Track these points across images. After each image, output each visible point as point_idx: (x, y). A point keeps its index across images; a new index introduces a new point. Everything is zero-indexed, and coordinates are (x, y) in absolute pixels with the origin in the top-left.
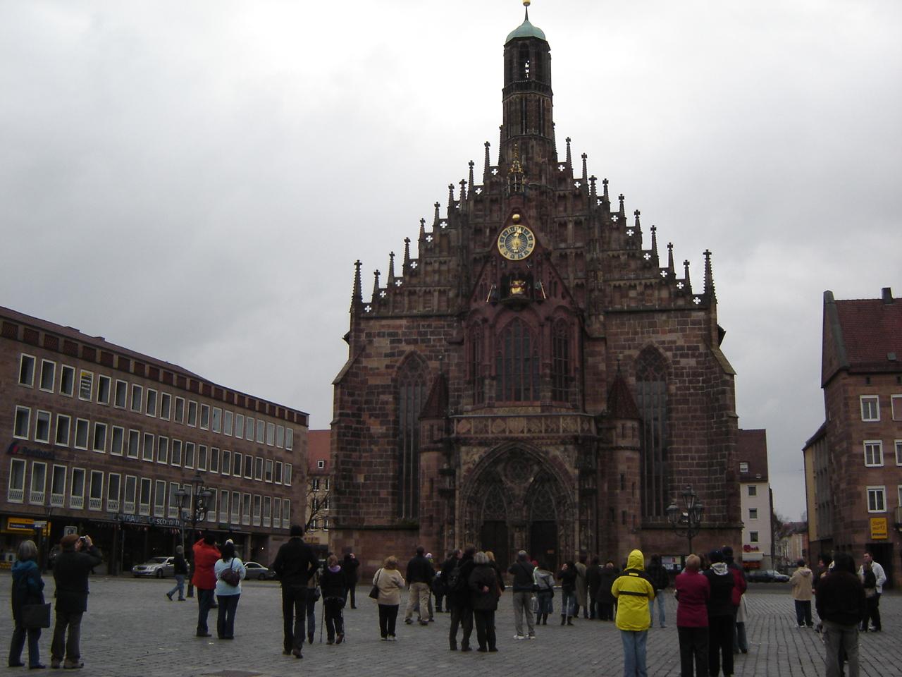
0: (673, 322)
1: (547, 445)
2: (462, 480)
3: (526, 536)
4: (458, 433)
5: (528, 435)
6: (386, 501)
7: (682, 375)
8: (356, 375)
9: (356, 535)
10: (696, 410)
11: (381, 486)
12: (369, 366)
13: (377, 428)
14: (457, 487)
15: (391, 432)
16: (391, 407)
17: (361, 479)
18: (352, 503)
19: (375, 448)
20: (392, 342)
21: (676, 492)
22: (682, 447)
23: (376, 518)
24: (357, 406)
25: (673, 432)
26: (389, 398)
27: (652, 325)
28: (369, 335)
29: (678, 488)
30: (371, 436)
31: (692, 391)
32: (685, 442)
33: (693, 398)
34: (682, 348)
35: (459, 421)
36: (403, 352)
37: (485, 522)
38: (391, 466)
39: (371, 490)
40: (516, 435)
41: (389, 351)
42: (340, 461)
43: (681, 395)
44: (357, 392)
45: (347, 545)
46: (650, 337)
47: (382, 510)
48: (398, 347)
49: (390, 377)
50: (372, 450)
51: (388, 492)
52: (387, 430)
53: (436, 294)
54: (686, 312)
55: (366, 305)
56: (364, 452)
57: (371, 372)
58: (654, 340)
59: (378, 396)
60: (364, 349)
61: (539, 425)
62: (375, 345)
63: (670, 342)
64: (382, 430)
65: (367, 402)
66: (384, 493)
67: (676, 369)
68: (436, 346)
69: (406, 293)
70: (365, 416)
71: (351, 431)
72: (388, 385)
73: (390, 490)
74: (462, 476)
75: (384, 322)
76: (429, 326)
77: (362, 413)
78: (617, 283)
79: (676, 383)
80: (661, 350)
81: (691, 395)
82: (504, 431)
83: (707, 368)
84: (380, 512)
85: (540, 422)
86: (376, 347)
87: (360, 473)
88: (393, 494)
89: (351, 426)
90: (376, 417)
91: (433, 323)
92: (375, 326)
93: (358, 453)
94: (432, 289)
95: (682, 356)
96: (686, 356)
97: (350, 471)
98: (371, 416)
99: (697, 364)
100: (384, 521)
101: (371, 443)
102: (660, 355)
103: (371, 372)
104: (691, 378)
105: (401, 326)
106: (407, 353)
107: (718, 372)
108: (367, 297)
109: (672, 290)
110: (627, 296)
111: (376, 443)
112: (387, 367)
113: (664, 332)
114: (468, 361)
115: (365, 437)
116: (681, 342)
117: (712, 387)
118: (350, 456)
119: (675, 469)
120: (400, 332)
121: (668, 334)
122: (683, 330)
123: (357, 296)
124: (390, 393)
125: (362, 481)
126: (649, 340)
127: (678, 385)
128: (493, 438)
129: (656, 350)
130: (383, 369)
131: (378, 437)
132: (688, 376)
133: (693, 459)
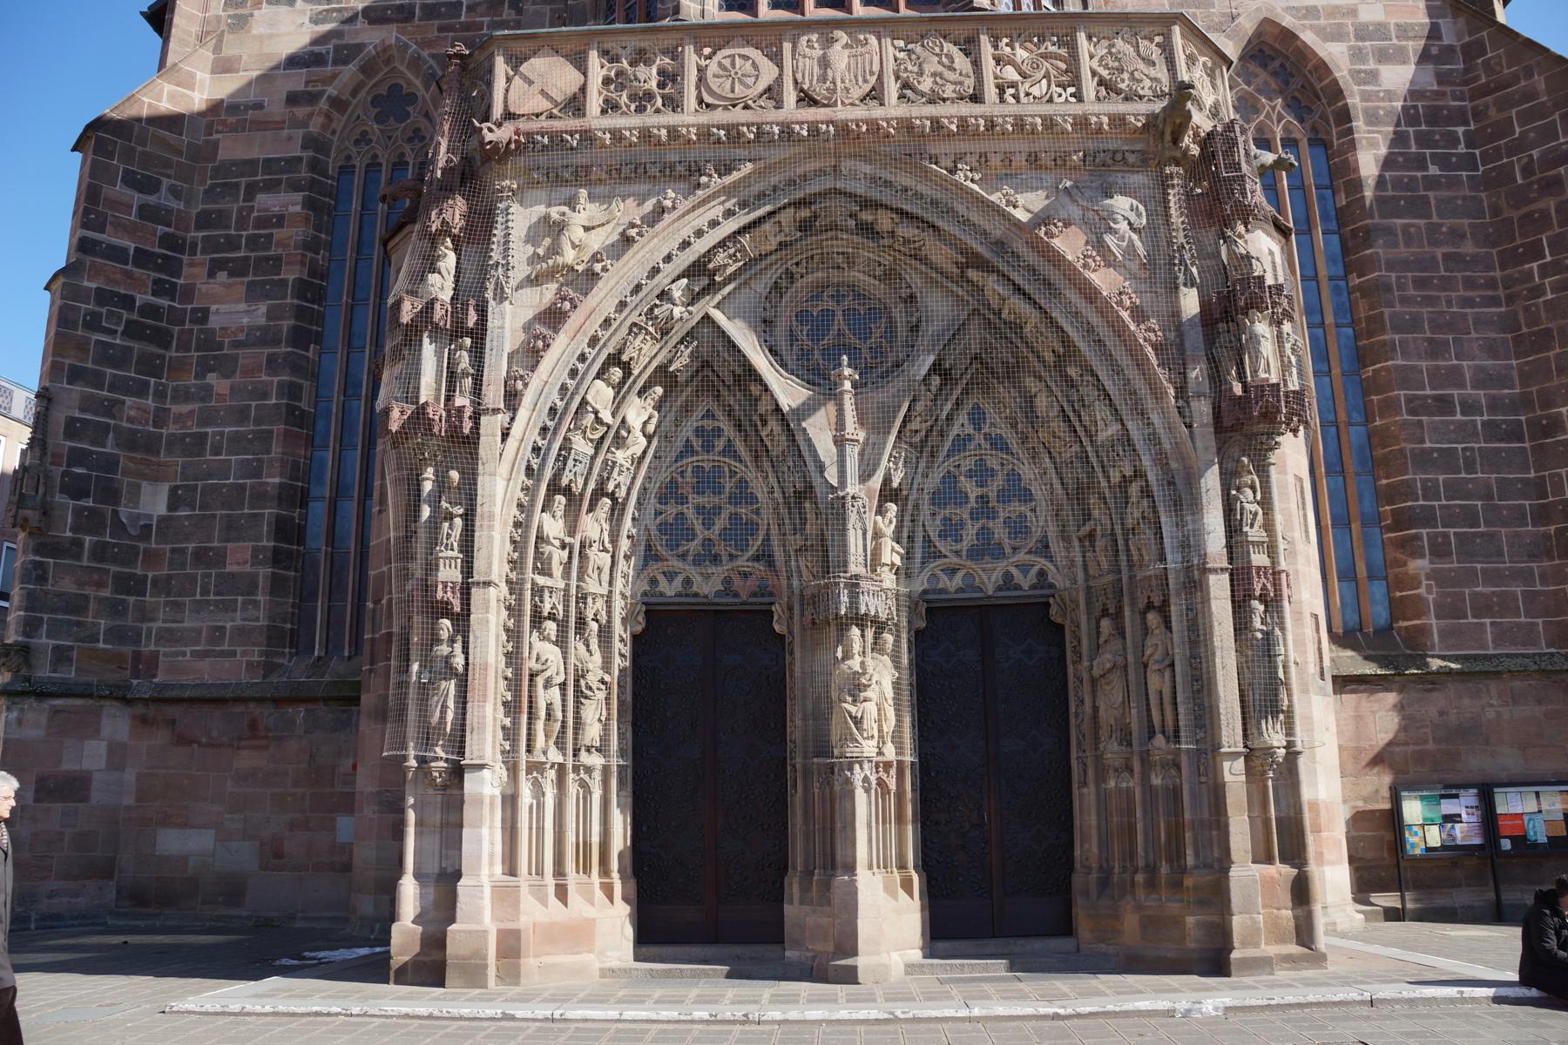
4: (509, 116)
9: (116, 723)
10: (1457, 235)
11: (232, 529)
13: (233, 310)
14: (493, 394)
15: (286, 324)
16: (293, 234)
17: (154, 502)
18: (106, 593)
19: (218, 384)
22: (1424, 364)
25: (1387, 311)
26: (289, 203)
30: (209, 342)
31: (1433, 170)
33: (1445, 194)
34: (1380, 31)
35: (516, 62)
36: (360, 47)
38: (276, 450)
39: (191, 546)
40: (842, 113)
42: (59, 416)
44: (165, 182)
45: (68, 766)
49: (301, 131)
50: (209, 388)
51: (256, 550)
52: (271, 315)
56: (175, 400)
57: (231, 120)
59: (250, 196)
61: (962, 62)
62: (254, 32)
65: (204, 221)
66: (239, 558)
67: (1366, 97)
68: (480, 26)
70: (193, 272)
71: (125, 315)
72: (289, 161)
77: (185, 258)
80: (1308, 37)
81: (1432, 183)
82: (773, 93)
86: (261, 38)
87: (156, 479)
88: (277, 558)
89: (132, 299)
90: (231, 274)
93: (150, 402)
97: (110, 464)
98: (215, 268)
99: (1440, 83)
100: (236, 667)
101: (204, 368)
103: (231, 120)
111: (226, 366)
112: (293, 99)
118: (110, 408)
124: (295, 187)
125: (161, 509)
128: (705, 133)
129: (1288, 36)
131: (237, 344)
133: (1469, 408)
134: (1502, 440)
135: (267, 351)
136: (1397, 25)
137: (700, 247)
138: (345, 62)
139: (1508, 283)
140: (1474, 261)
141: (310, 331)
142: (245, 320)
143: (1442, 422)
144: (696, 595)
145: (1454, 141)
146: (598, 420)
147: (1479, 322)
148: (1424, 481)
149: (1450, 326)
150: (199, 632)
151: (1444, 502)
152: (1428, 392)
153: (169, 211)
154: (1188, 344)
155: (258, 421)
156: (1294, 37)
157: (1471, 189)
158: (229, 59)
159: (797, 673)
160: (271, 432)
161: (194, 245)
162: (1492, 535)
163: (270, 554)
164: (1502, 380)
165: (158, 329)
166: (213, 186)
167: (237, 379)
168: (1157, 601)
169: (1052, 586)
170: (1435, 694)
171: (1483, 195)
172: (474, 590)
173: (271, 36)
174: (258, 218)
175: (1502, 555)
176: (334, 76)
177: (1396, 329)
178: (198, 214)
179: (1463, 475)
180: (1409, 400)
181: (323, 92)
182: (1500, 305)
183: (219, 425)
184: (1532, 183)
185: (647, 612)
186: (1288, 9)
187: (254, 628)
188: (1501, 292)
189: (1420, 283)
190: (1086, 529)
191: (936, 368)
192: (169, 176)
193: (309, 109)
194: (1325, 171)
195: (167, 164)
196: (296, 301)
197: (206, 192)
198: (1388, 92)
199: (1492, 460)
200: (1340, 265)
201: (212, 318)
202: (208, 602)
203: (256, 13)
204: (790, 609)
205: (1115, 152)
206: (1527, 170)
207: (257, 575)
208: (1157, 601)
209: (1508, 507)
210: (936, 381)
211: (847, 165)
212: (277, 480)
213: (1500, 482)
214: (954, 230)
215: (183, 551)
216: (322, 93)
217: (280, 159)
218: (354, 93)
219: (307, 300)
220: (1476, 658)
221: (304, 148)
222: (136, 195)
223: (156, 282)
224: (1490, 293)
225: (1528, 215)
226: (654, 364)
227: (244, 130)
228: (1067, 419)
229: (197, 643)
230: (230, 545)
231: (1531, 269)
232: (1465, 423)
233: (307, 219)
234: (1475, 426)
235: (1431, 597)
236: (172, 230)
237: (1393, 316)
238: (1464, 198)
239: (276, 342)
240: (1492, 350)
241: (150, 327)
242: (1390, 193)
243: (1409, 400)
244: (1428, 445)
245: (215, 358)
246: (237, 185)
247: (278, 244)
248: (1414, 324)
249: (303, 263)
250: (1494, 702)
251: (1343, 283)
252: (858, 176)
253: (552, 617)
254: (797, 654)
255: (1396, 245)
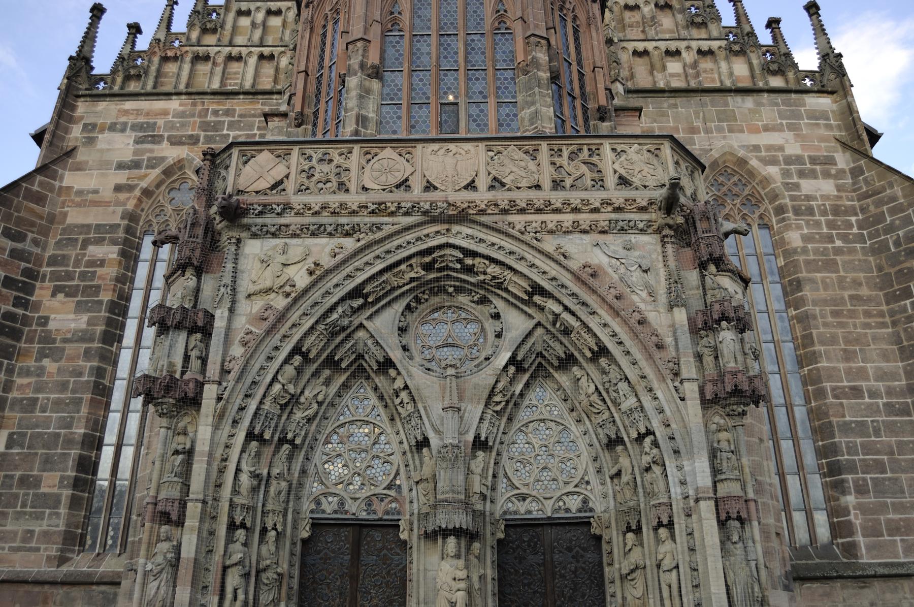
0: (768, 110)
1: (559, 230)
2: (237, 351)
3: (482, 578)
5: (490, 195)
6: (54, 501)
7: (810, 211)
8: (40, 199)
10: (857, 283)
11: (48, 463)
12: (76, 187)
14: (213, 370)
15: (100, 329)
16: (110, 272)
20: (138, 141)
21: (850, 477)
22: (841, 366)
23: (18, 549)
24: (23, 265)
25: (814, 332)
27: (727, 116)
28: (90, 128)
29: (852, 468)
30: (47, 339)
31: (839, 243)
32: (848, 356)
33: (847, 258)
34: (799, 160)
36: (163, 159)
37: (316, 525)
38: (84, 410)
39: (18, 474)
41: (128, 157)
43: (816, 251)
44: (30, 235)
46: (725, 137)
47: (38, 527)
48: (152, 151)
50: (41, 371)
51: (62, 478)
52: (89, 323)
53: (253, 61)
54: (793, 96)
55: (101, 78)
56: (20, 375)
57: (78, 199)
58: (736, 145)
60: (70, 153)
62: (98, 147)
63: (769, 148)
64: (81, 322)
67: (793, 198)
69: (188, 58)
70: (42, 293)
72: (111, 226)
73: (71, 473)
74: (239, 336)
75: (129, 105)
76: (228, 113)
77: (38, 284)
78: (640, 46)
79: (799, 227)
80: (754, 163)
81: (838, 251)
83: (866, 196)
84: (32, 532)
85: (533, 155)
86: (102, 151)
90: (67, 295)
91: (237, 108)
92: (107, 110)
94: (244, 51)
95: (802, 174)
96: (813, 175)
99: (838, 191)
101: (42, 355)
102: (752, 174)
103: (78, 199)
104: (830, 217)
105: (165, 113)
106: (171, 161)
107: (900, 193)
108: (102, 63)
109: (755, 62)
110: (664, 68)
111: (55, 354)
112: (118, 188)
113: (755, 130)
114: (302, 68)
115: (30, 341)
116: (793, 149)
117: (890, 229)
119: (834, 420)
120: (160, 122)
121: (763, 133)
122: (792, 128)
123: (81, 62)
124: (114, 242)
126: (723, 143)
127: (806, 231)
130: (107, 193)
131: (65, 341)
132: (824, 213)
133: (873, 394)
134: (897, 415)
135: (85, 345)
136: (810, 157)
137: (361, 278)
138: (153, 167)
139: (892, 313)
140: (869, 300)
141: (115, 334)
142: (73, 325)
143: (856, 403)
144: (346, 512)
145: (851, 226)
146: (286, 391)
147: (875, 338)
148: (847, 443)
149: (857, 341)
150: (15, 533)
151: (861, 457)
152: (845, 384)
153: (30, 254)
154: (680, 345)
155: (74, 391)
156: (746, 162)
157: (864, 255)
158: (80, 163)
159: (414, 571)
160: (81, 399)
161: (44, 276)
162: (896, 479)
163: (72, 481)
164: (893, 376)
165: (13, 330)
166: (61, 240)
167: (63, 363)
168: (665, 521)
169: (591, 510)
170: (866, 591)
171: (871, 259)
172: (189, 504)
173: (108, 150)
174: (89, 260)
175: (903, 492)
176: (146, 176)
177: (822, 343)
178: (50, 257)
179: (873, 439)
180: (833, 389)
181: (137, 185)
182: (888, 327)
183: (47, 393)
184: (901, 251)
185: (313, 525)
186: (740, 147)
187: (55, 532)
188: (888, 320)
189: (835, 314)
190: (614, 471)
191: (512, 361)
192: (33, 232)
193: (128, 195)
194: (770, 244)
195: (33, 224)
196: (107, 314)
197: (56, 243)
198: (806, 196)
199: (891, 428)
200: (783, 303)
201: (51, 323)
202: (25, 513)
203: (100, 136)
204: (411, 524)
205: (629, 221)
206: (897, 243)
207: (60, 495)
208: (665, 521)
209: (905, 460)
210: (512, 369)
211: (456, 228)
212: (82, 431)
213: (899, 444)
214: (526, 271)
215: (12, 477)
216: (137, 185)
217: (106, 225)
218: (158, 186)
219: (115, 314)
220: (892, 565)
221: (122, 218)
222: (10, 243)
223: (16, 298)
224: (881, 320)
225: (901, 271)
226: (325, 355)
227: (85, 206)
228: (600, 394)
229: (15, 541)
230: (45, 474)
231: (906, 305)
232: (872, 404)
233: (120, 262)
234: (878, 406)
235: (858, 522)
236: (30, 266)
237: (819, 335)
238: (860, 260)
239: (92, 340)
240: (885, 356)
241: (8, 327)
242: (812, 257)
243: (833, 389)
244: (848, 418)
245: (50, 349)
246: (77, 240)
247: (99, 278)
248: (833, 340)
249: (114, 290)
250: (908, 596)
251: (785, 314)
252: (462, 236)
253: (243, 525)
254: (415, 555)
255: (818, 290)
